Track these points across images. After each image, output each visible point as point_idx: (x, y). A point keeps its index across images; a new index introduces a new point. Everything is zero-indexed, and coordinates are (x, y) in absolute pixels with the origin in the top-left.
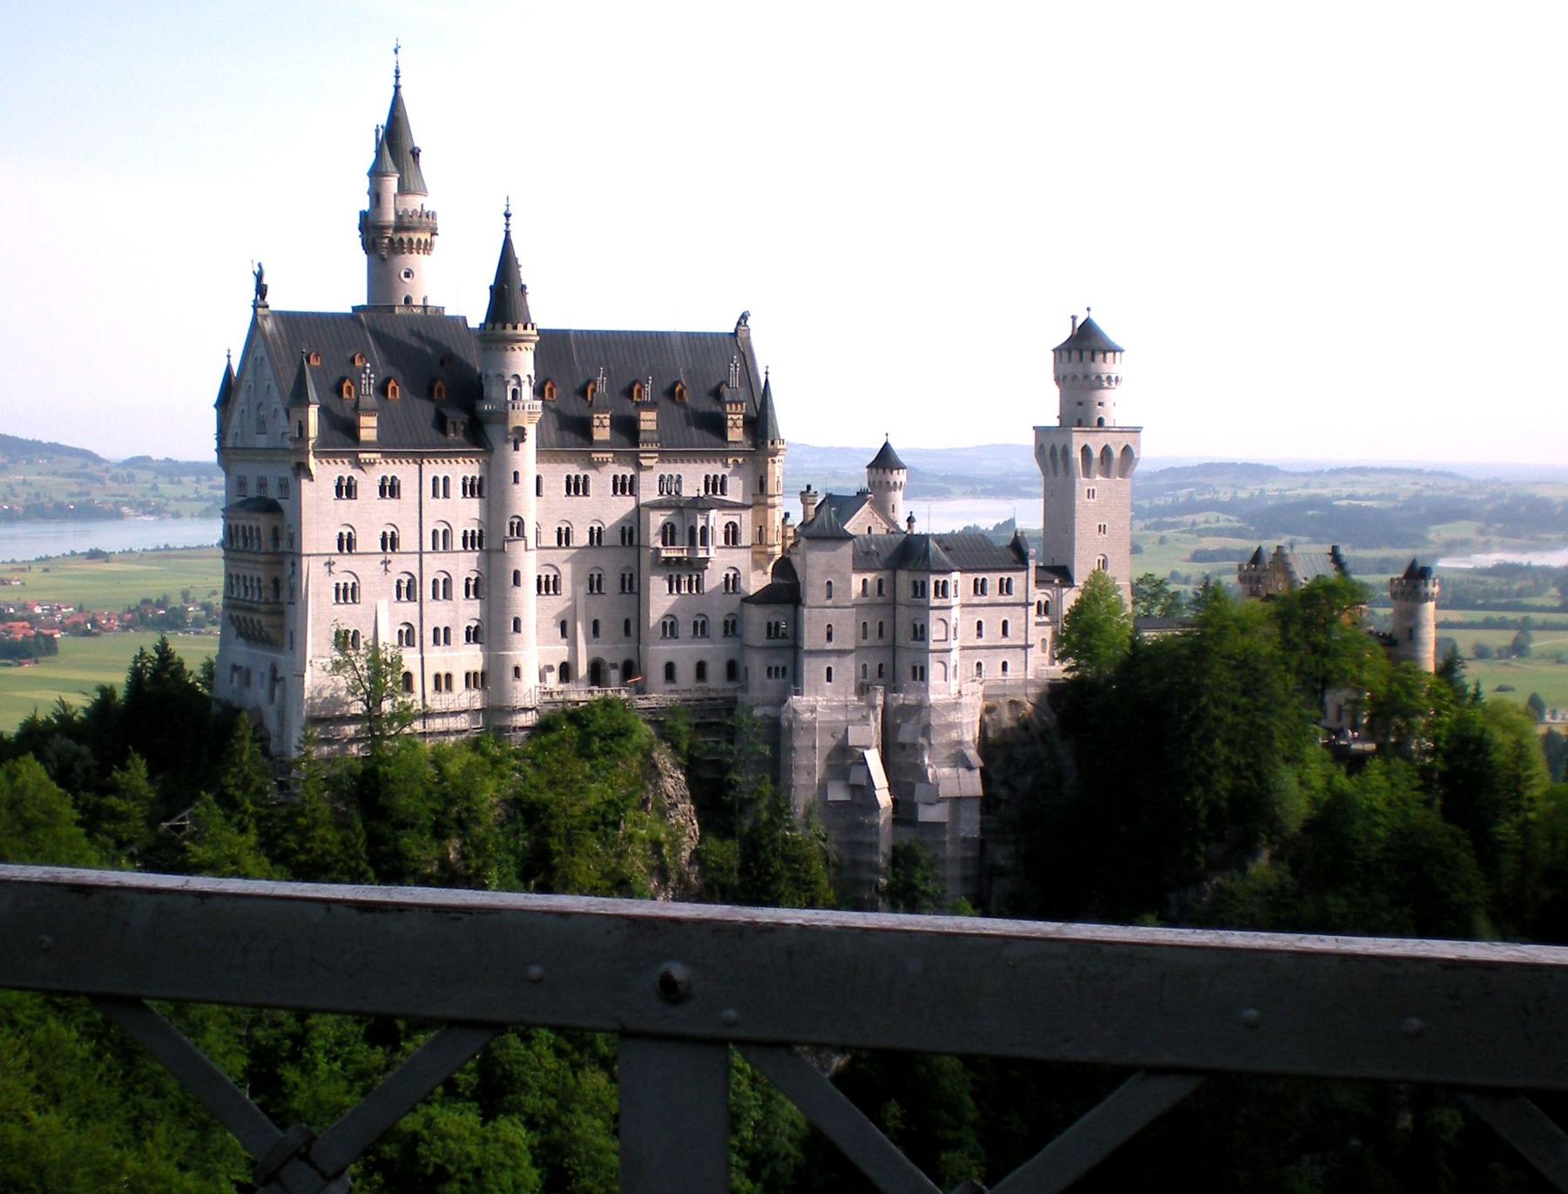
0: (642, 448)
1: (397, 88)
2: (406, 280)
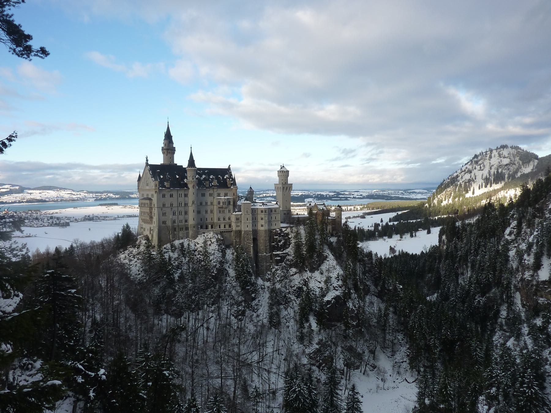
1: (168, 125)
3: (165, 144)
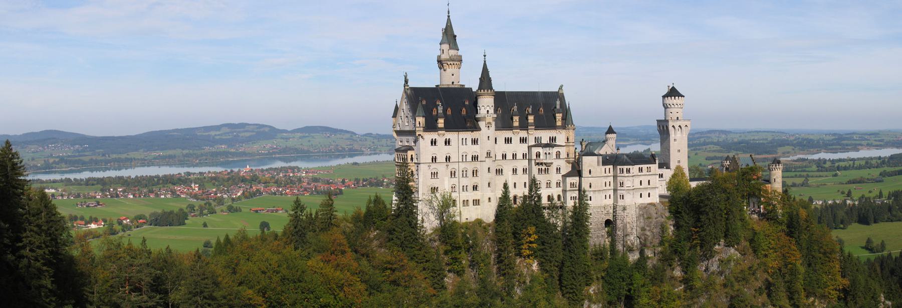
0: (529, 128)
1: (449, 16)
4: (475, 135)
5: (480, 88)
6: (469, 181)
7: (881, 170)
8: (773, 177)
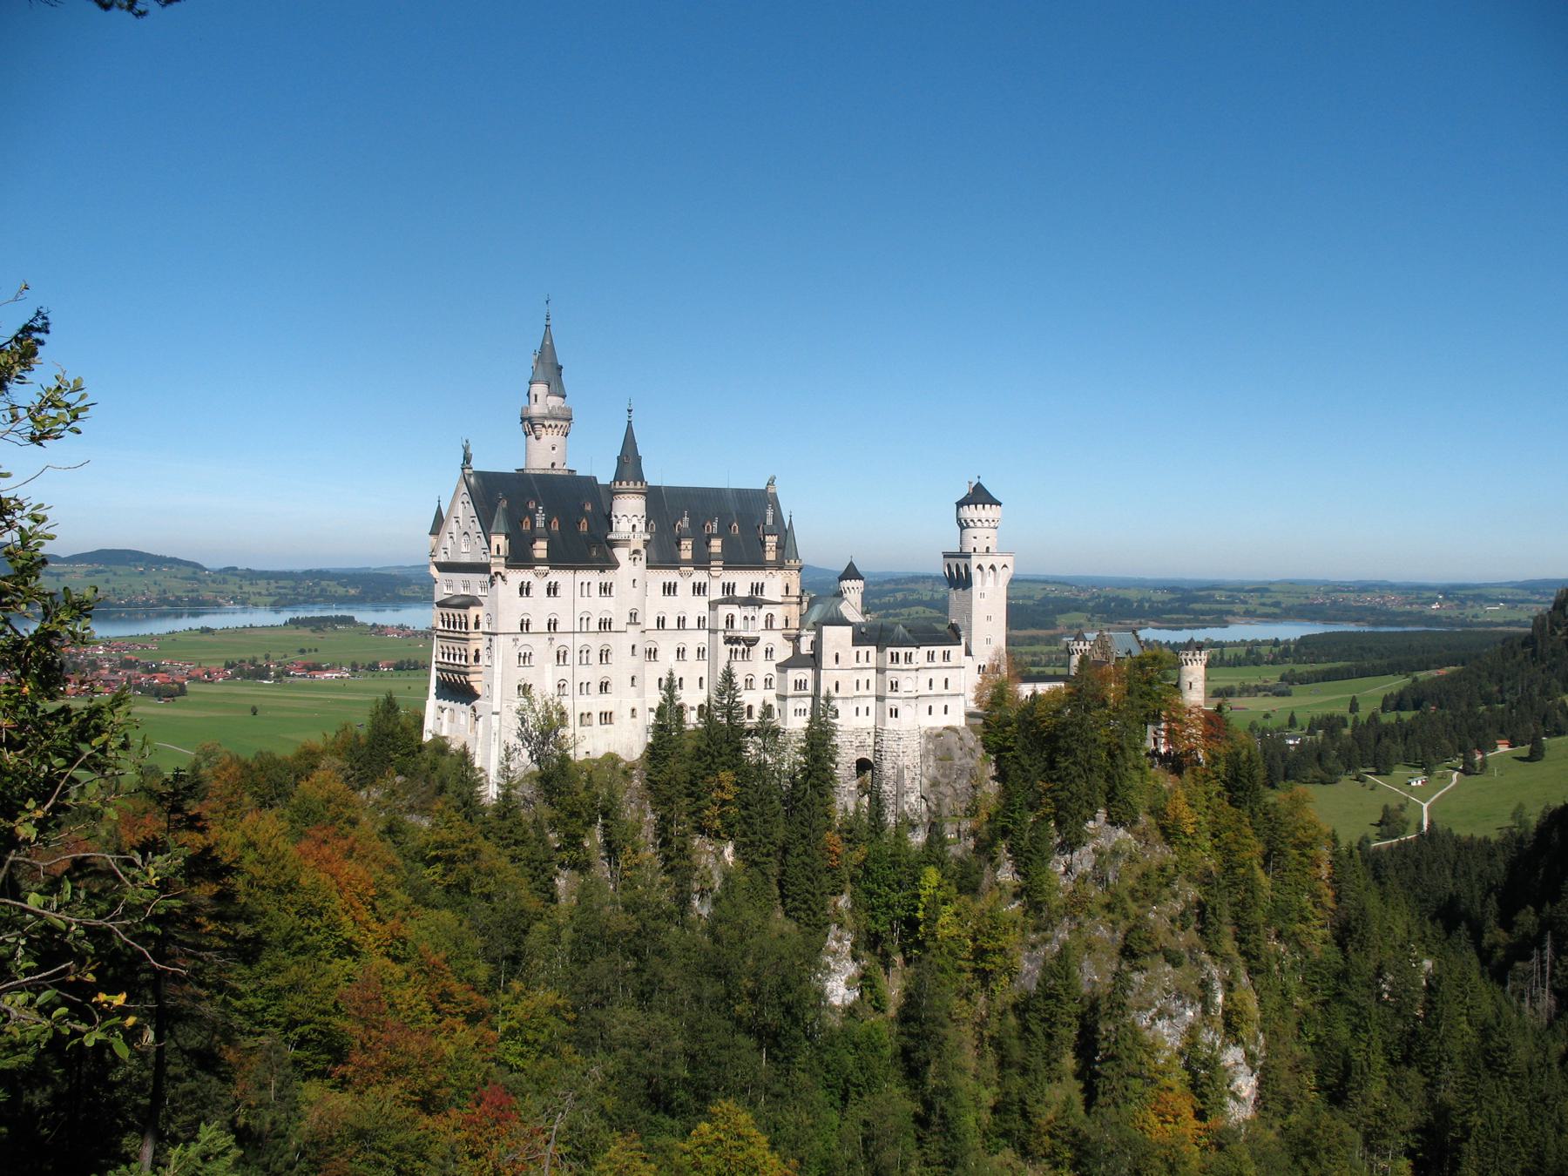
0: (712, 564)
2: (554, 452)
3: (536, 396)
4: (608, 576)
5: (619, 477)
6: (593, 673)
7: (1285, 669)
8: (1186, 679)
